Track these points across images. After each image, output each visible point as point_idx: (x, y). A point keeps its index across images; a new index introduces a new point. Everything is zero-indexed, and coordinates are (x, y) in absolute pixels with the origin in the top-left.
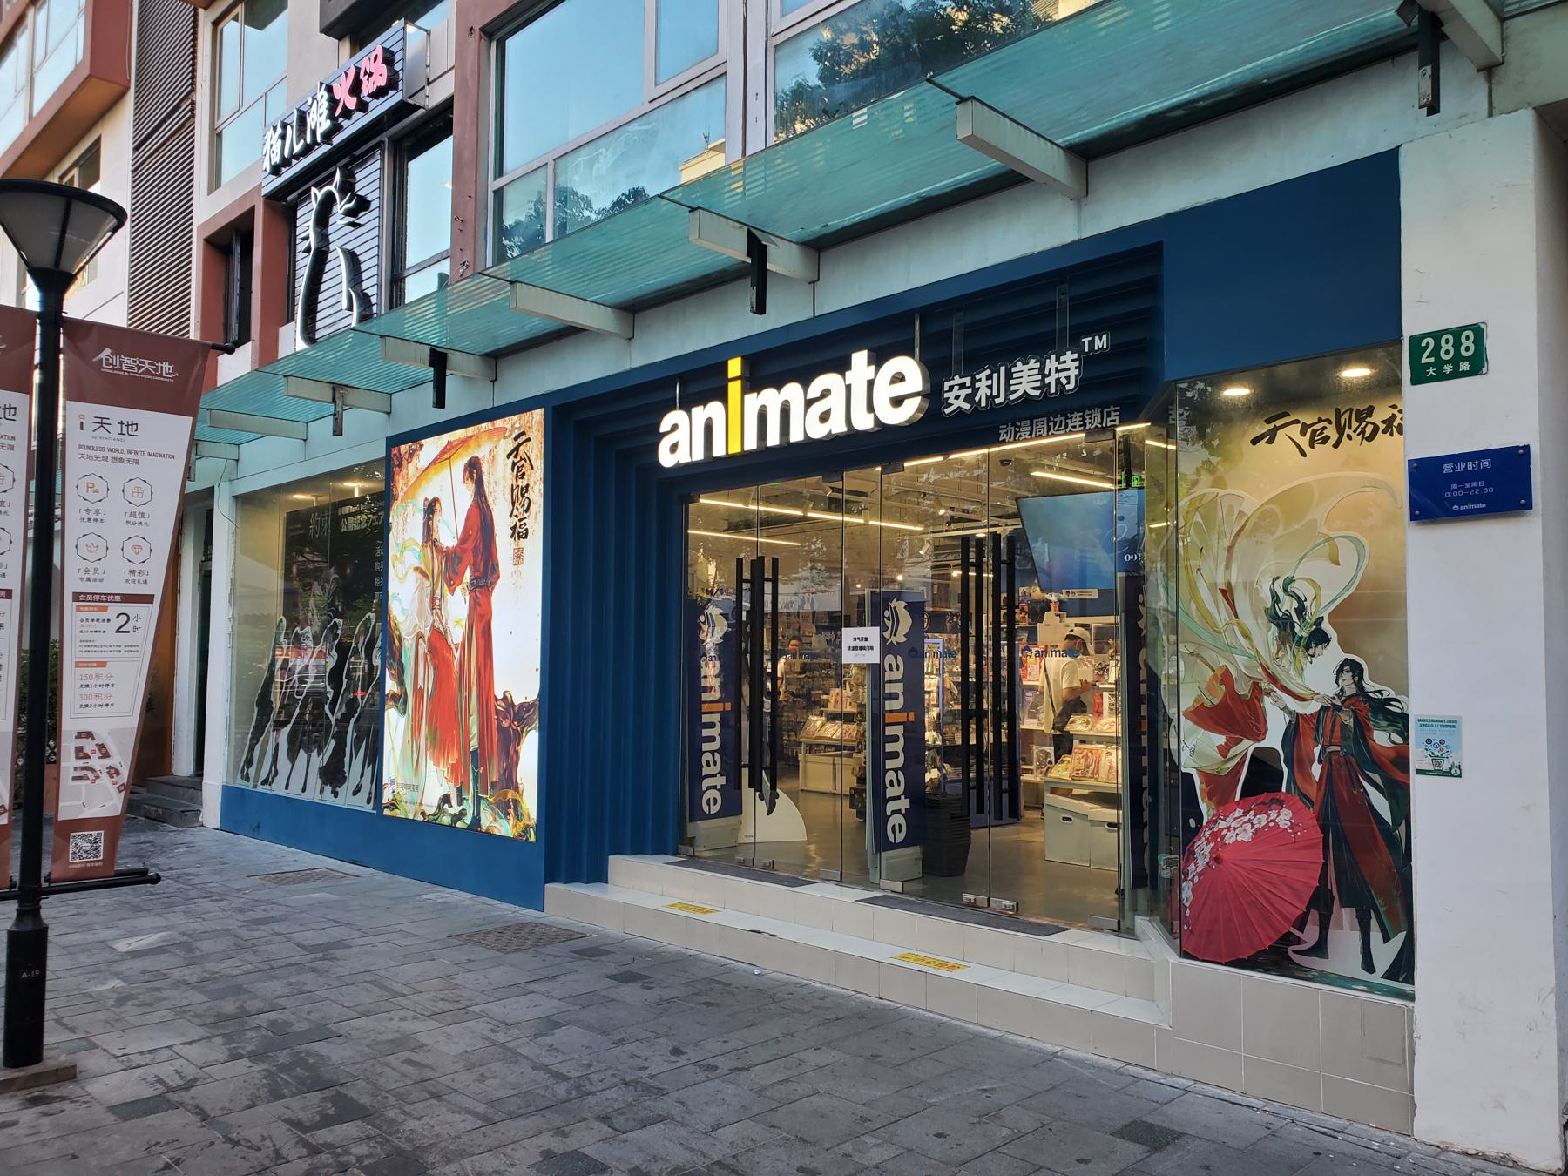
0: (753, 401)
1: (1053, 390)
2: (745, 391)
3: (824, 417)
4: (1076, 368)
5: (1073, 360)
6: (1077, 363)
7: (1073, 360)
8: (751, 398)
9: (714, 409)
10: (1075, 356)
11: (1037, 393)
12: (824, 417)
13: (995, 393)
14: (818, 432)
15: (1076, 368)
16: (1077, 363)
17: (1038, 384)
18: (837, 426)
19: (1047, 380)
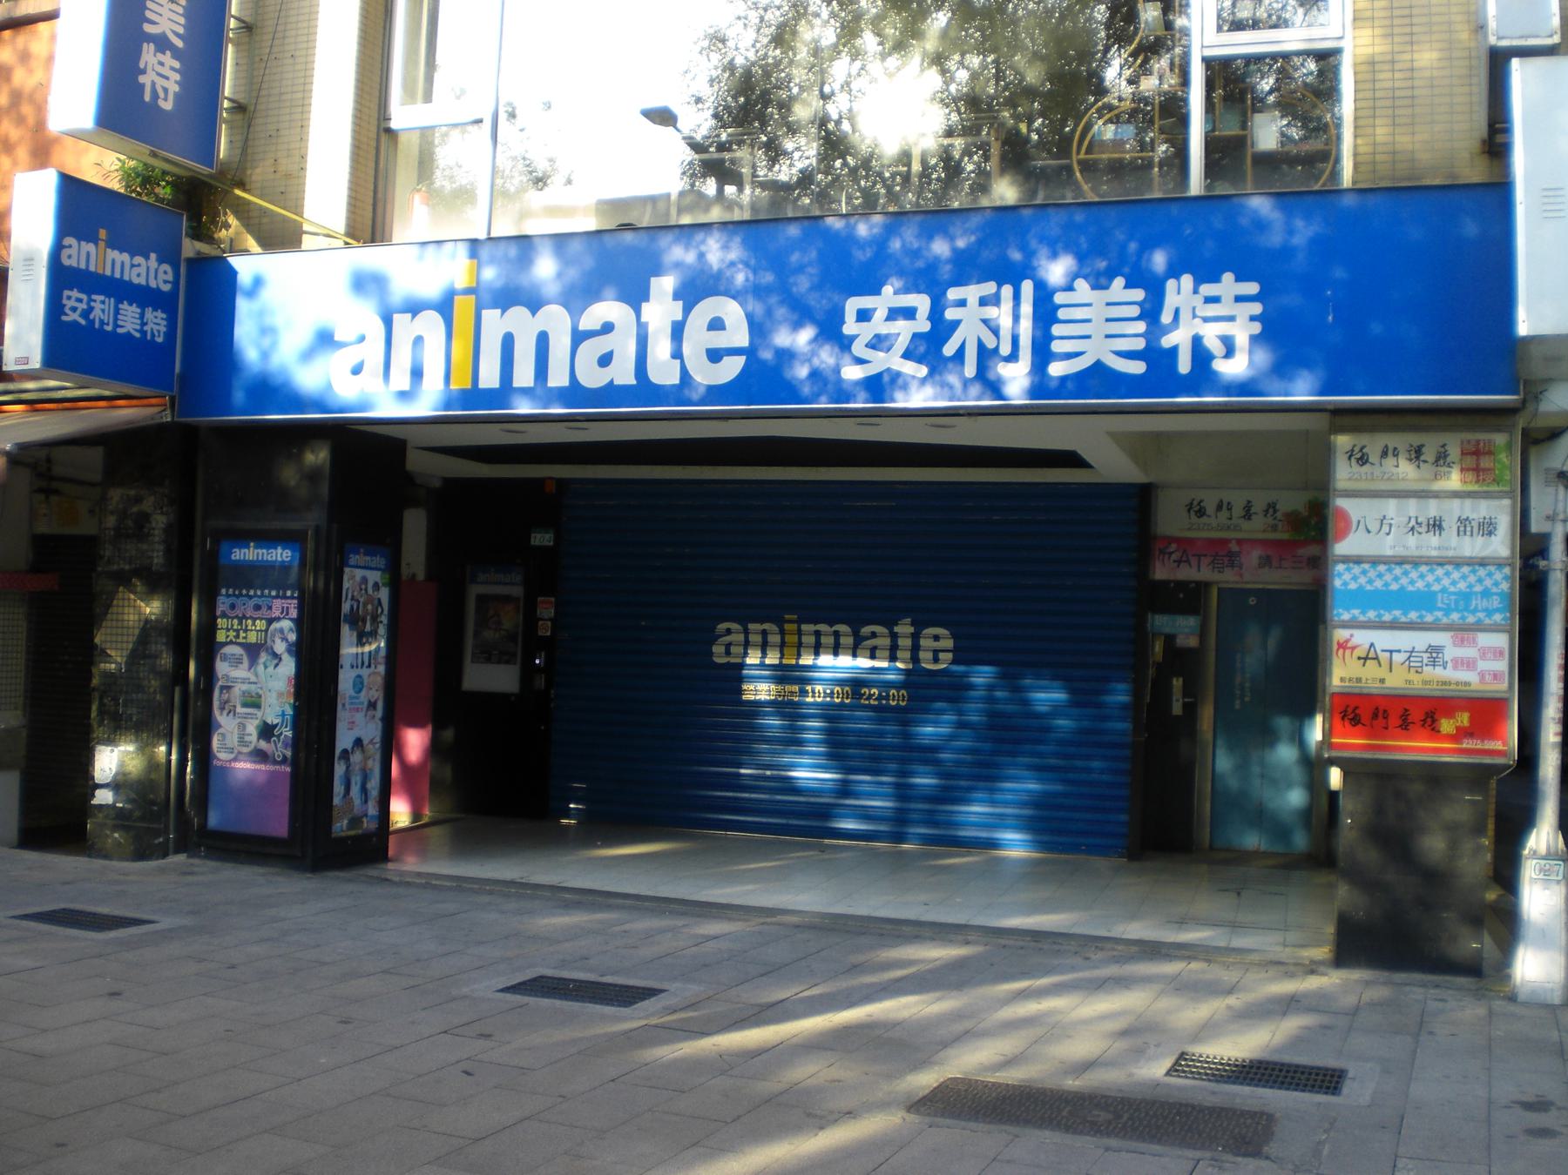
1: (1184, 366)
3: (605, 360)
4: (1253, 318)
5: (1239, 299)
6: (1257, 308)
7: (1239, 299)
10: (1252, 288)
11: (1137, 368)
12: (605, 360)
13: (1005, 350)
14: (592, 378)
15: (1253, 318)
16: (1257, 308)
17: (1140, 344)
18: (623, 373)
19: (1167, 341)
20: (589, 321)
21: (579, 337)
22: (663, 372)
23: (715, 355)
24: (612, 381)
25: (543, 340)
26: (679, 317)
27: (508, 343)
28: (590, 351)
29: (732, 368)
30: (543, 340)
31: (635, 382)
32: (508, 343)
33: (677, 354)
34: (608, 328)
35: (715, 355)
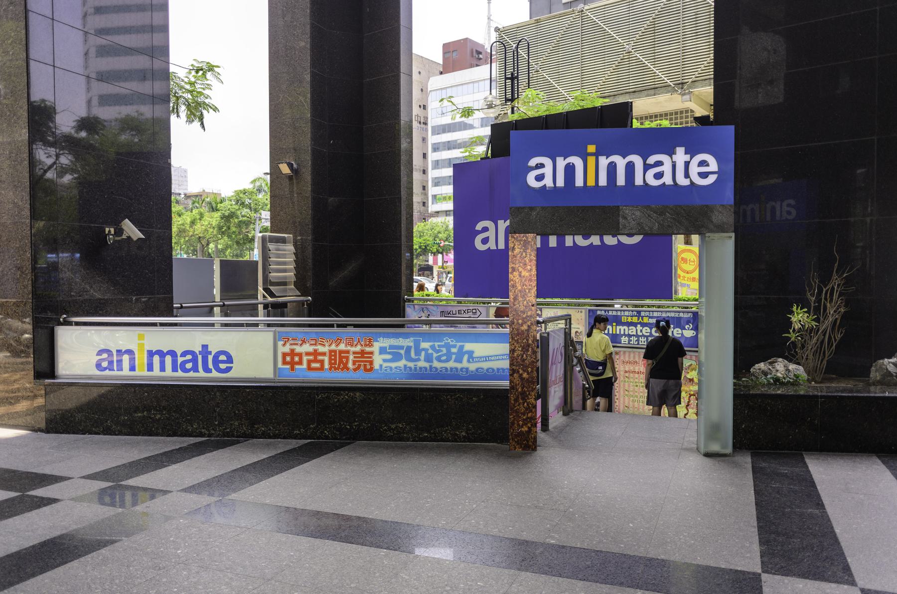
0: (604, 162)
2: (597, 155)
3: (658, 176)
9: (577, 161)
12: (658, 176)
14: (653, 182)
20: (652, 160)
21: (647, 167)
22: (682, 181)
23: (703, 175)
24: (664, 182)
25: (630, 167)
26: (689, 160)
27: (612, 168)
28: (651, 173)
30: (630, 167)
31: (672, 184)
32: (612, 168)
33: (687, 175)
34: (659, 163)
35: (703, 175)
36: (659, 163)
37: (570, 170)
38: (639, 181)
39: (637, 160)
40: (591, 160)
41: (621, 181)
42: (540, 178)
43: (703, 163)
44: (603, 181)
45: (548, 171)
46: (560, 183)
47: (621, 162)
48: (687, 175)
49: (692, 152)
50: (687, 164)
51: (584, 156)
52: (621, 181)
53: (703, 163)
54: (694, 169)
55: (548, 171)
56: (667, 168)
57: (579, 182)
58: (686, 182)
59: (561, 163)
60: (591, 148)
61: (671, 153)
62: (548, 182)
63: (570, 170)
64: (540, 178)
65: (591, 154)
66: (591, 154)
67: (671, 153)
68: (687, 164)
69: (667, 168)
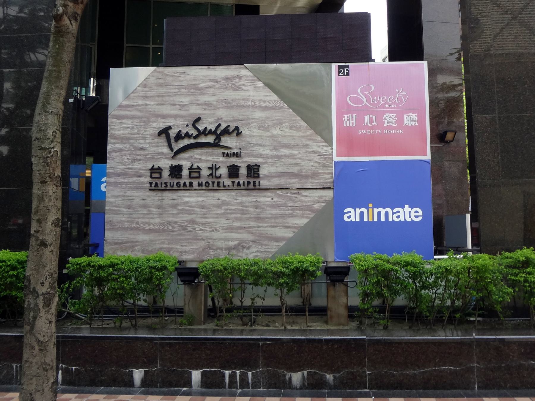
0: (376, 211)
2: (373, 208)
3: (398, 217)
8: (375, 209)
9: (364, 210)
14: (397, 220)
18: (402, 219)
20: (395, 210)
21: (393, 213)
25: (387, 213)
27: (379, 213)
29: (420, 219)
30: (387, 213)
32: (379, 213)
33: (410, 217)
34: (398, 212)
36: (398, 212)
37: (362, 214)
38: (390, 219)
39: (389, 210)
40: (370, 210)
41: (383, 219)
42: (349, 217)
43: (416, 212)
44: (376, 219)
45: (352, 214)
46: (358, 219)
47: (383, 211)
48: (410, 217)
49: (412, 207)
50: (410, 212)
51: (368, 208)
52: (383, 219)
53: (416, 212)
54: (413, 214)
55: (352, 214)
56: (402, 214)
57: (366, 219)
58: (409, 220)
59: (358, 211)
60: (370, 205)
61: (403, 207)
62: (353, 219)
63: (362, 214)
64: (349, 217)
65: (370, 208)
66: (370, 208)
67: (403, 207)
68: (410, 212)
69: (402, 214)
